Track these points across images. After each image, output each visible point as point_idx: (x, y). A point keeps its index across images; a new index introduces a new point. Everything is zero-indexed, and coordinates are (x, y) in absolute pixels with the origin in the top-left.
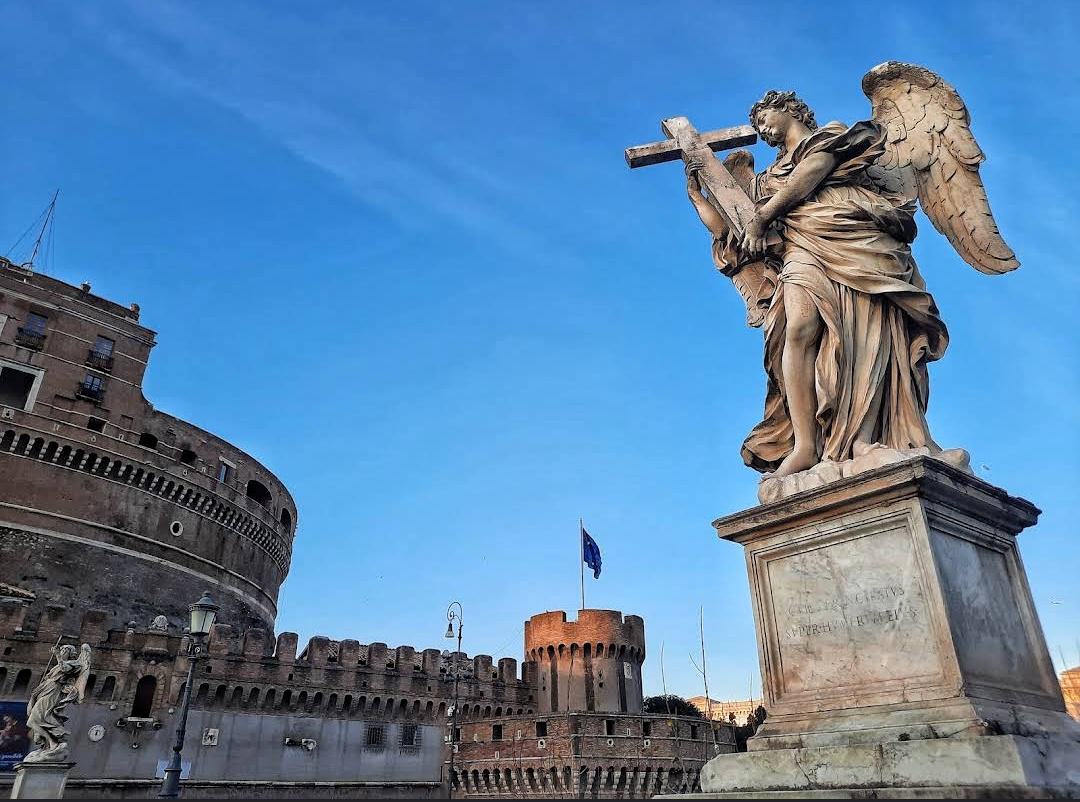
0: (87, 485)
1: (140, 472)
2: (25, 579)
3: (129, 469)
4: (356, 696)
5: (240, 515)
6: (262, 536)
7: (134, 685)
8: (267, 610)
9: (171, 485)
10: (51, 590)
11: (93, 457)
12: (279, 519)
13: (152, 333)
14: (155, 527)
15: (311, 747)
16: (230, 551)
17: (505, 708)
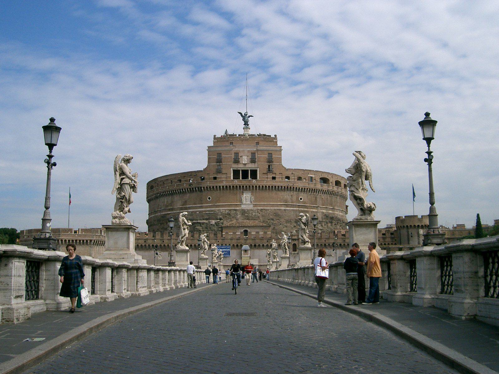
1: (288, 187)
2: (269, 220)
3: (285, 187)
4: (342, 244)
5: (319, 190)
6: (329, 193)
7: (292, 245)
8: (337, 213)
9: (296, 188)
10: (275, 221)
11: (275, 187)
12: (334, 185)
13: (281, 147)
14: (295, 200)
15: (333, 256)
16: (319, 200)
17: (387, 243)
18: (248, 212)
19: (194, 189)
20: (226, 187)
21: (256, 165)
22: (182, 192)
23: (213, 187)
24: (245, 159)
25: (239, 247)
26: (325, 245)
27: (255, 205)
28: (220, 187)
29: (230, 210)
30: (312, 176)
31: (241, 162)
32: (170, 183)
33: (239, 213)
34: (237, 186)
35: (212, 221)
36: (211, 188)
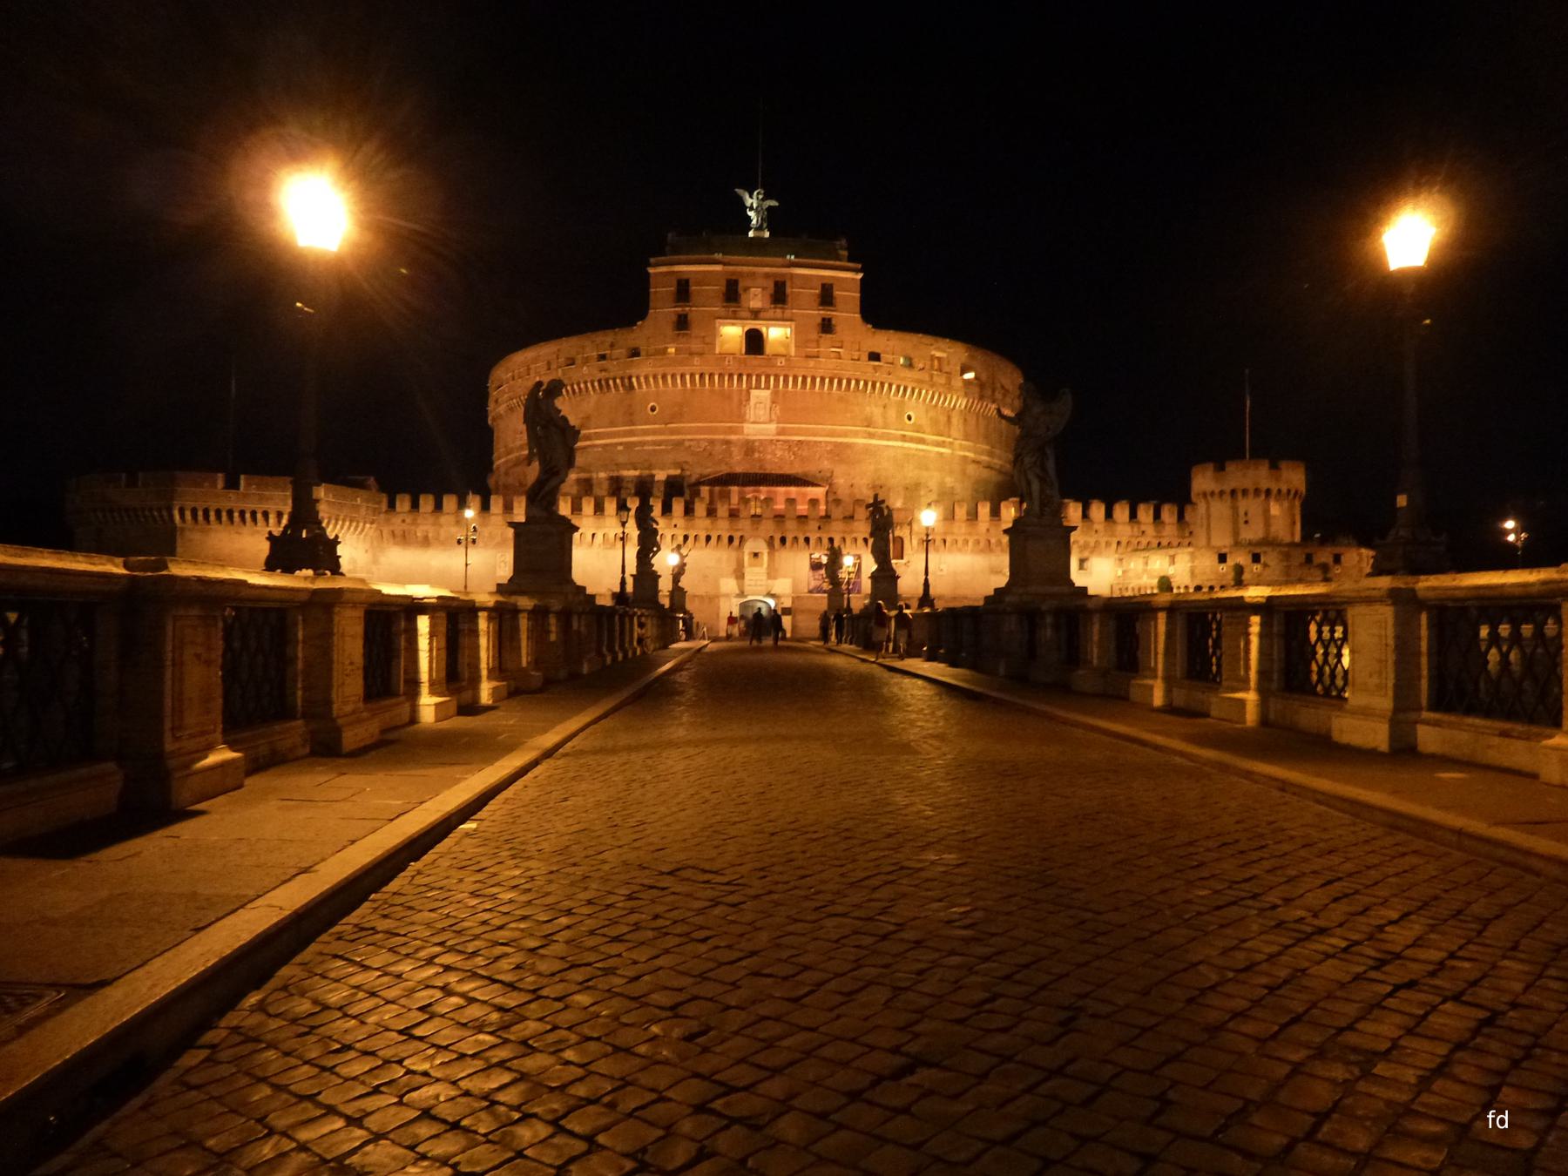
0: (841, 399)
18: (761, 449)
19: (611, 382)
20: (702, 375)
21: (788, 313)
22: (577, 390)
23: (664, 377)
24: (756, 298)
25: (736, 542)
26: (989, 541)
27: (781, 432)
28: (683, 376)
29: (712, 442)
30: (938, 354)
31: (744, 303)
32: (546, 367)
33: (735, 450)
34: (731, 376)
35: (661, 472)
36: (660, 377)
